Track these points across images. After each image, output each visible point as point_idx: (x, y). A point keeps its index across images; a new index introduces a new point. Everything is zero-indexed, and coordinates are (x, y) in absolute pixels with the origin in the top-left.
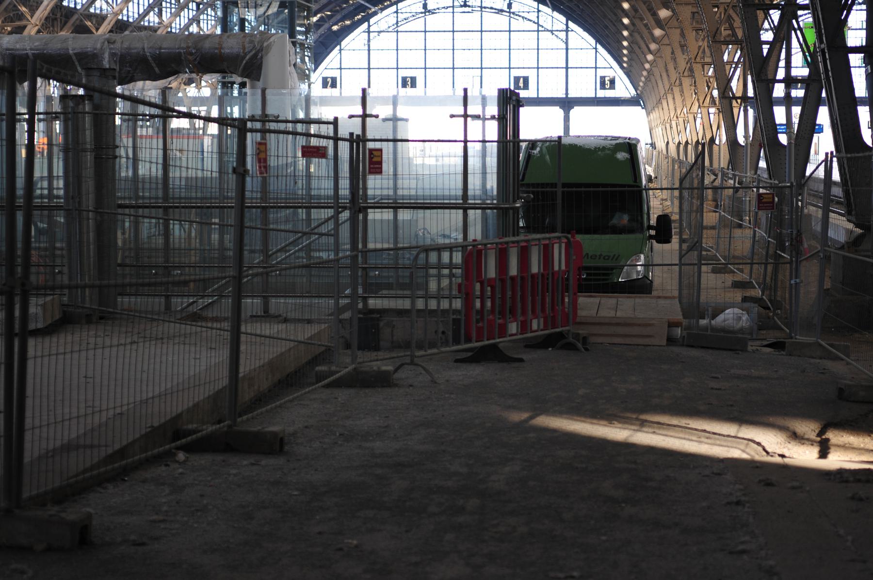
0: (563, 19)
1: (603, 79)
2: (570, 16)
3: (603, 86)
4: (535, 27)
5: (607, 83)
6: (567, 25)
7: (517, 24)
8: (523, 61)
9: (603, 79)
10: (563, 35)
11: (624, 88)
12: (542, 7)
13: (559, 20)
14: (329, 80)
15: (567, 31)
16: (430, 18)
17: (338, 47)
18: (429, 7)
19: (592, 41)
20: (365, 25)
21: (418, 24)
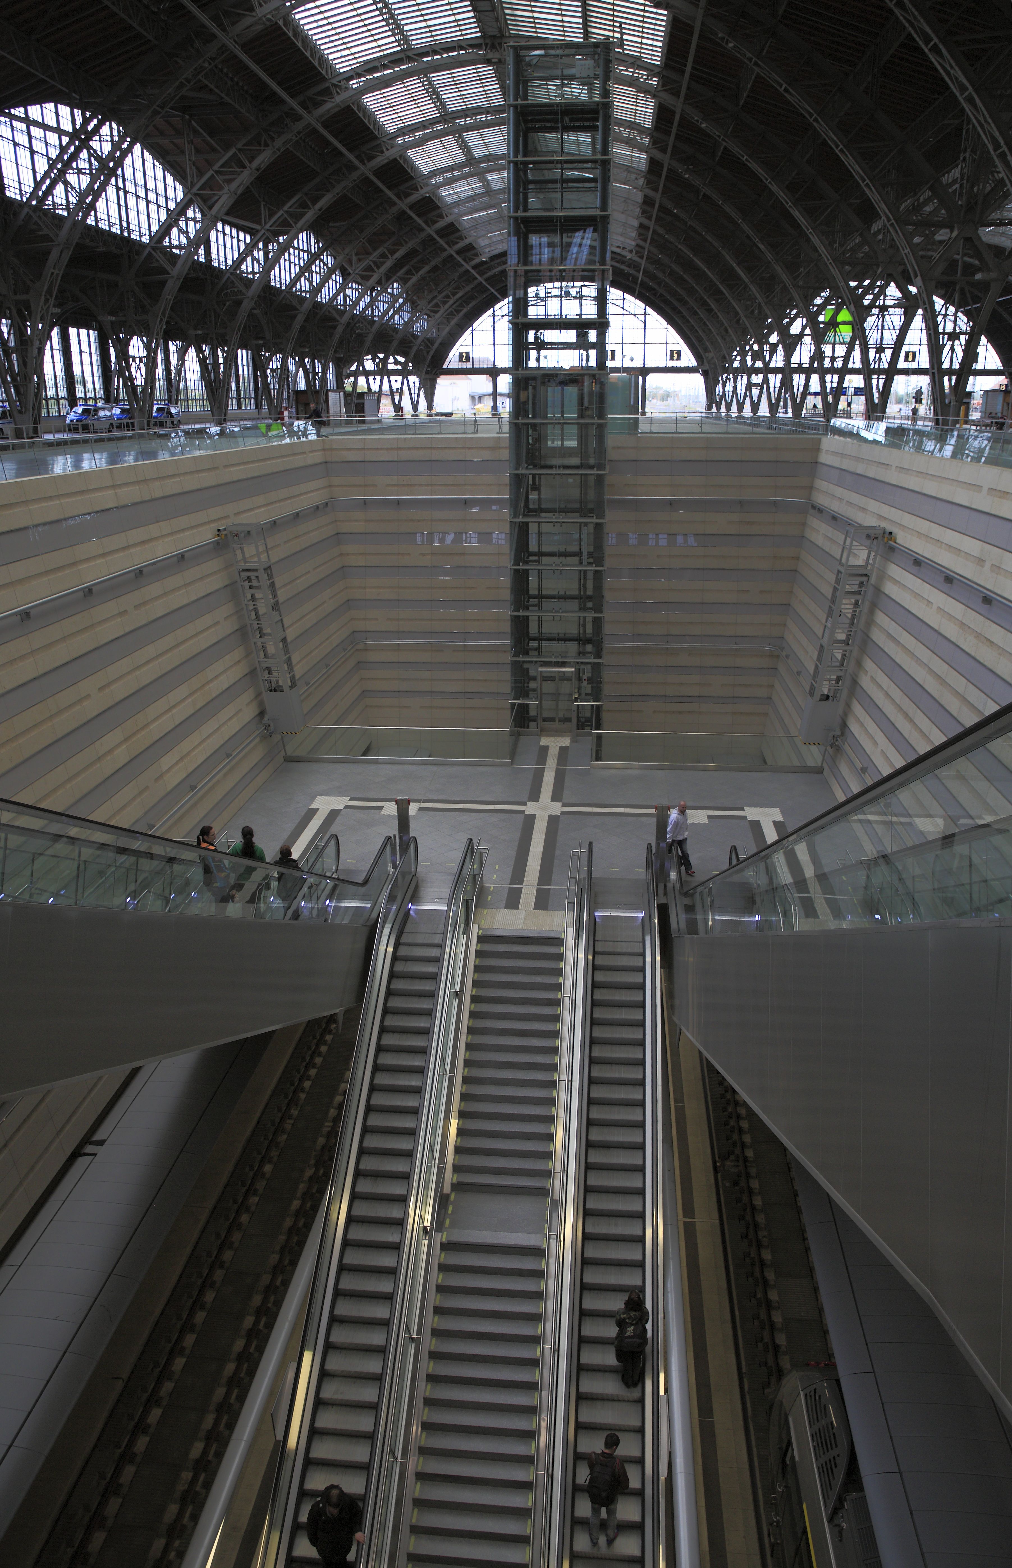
0: (642, 305)
1: (672, 352)
2: (648, 302)
3: (672, 358)
4: (620, 311)
5: (675, 355)
9: (672, 352)
11: (688, 359)
12: (627, 296)
13: (639, 306)
14: (464, 354)
15: (645, 314)
17: (470, 329)
19: (664, 323)
20: (491, 311)
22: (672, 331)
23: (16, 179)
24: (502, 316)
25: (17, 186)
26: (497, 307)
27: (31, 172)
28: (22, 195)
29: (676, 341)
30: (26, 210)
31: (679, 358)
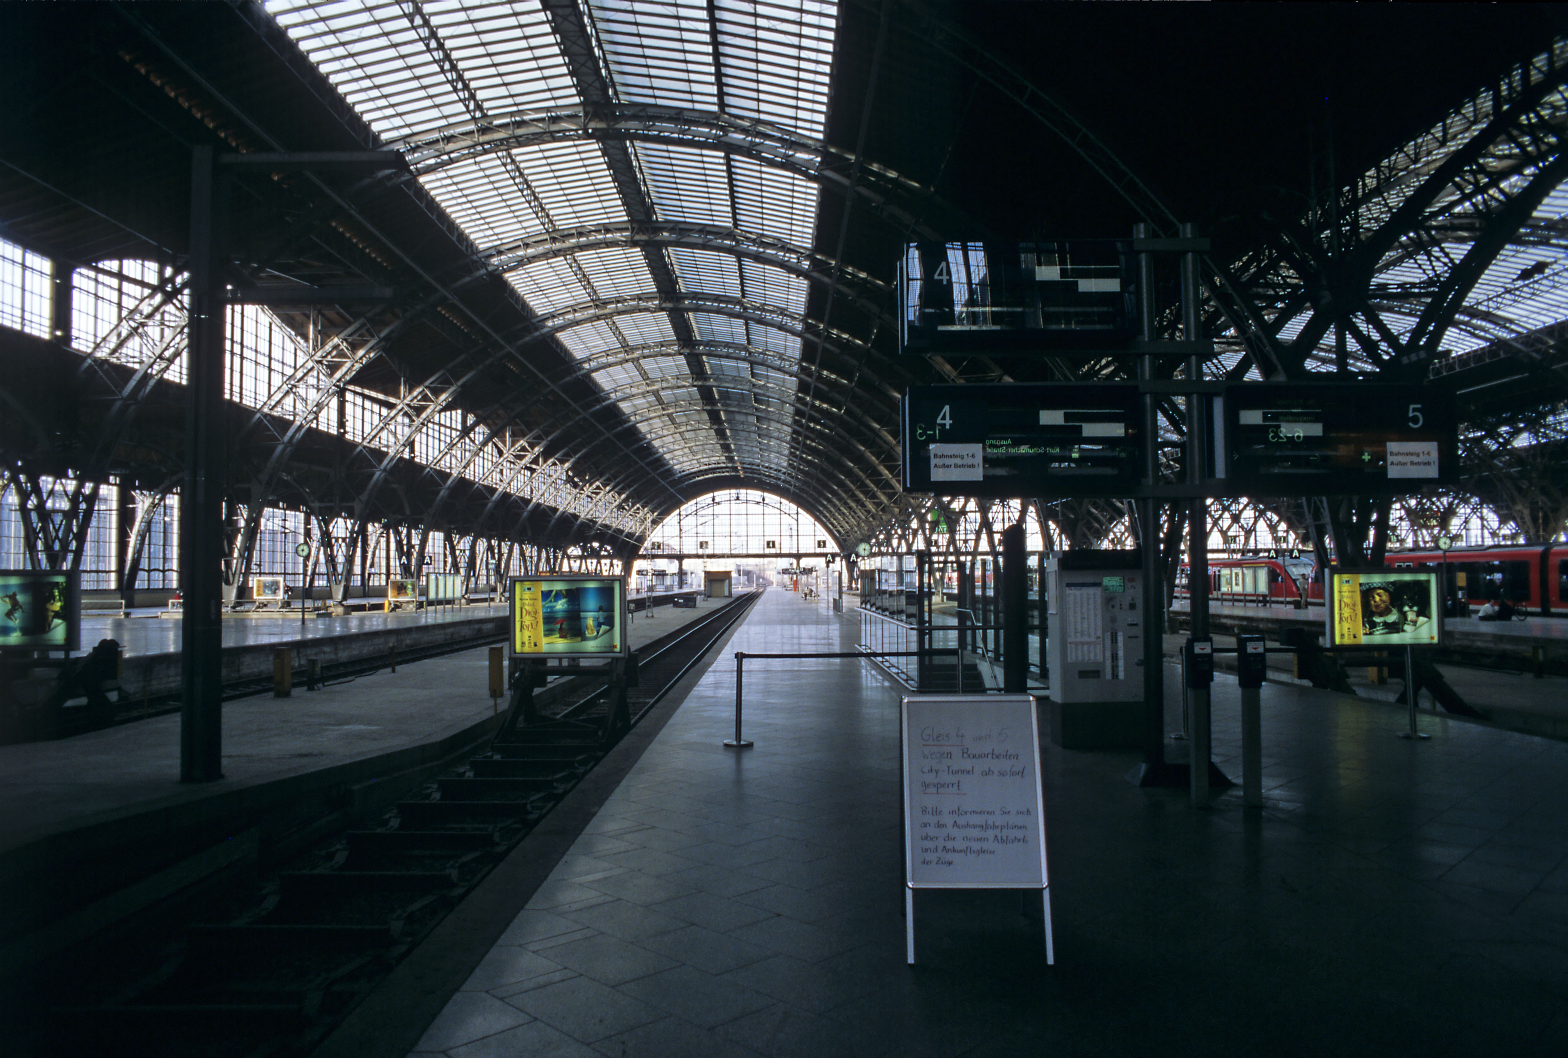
1: (819, 542)
3: (819, 546)
4: (778, 511)
5: (822, 544)
7: (768, 510)
9: (819, 542)
10: (795, 517)
12: (783, 500)
13: (793, 507)
15: (797, 514)
16: (717, 507)
18: (717, 500)
19: (812, 520)
20: (677, 511)
21: (709, 511)
22: (819, 527)
23: (253, 390)
24: (687, 516)
25: (253, 395)
26: (683, 508)
27: (267, 386)
28: (256, 403)
29: (822, 534)
30: (258, 415)
31: (824, 546)
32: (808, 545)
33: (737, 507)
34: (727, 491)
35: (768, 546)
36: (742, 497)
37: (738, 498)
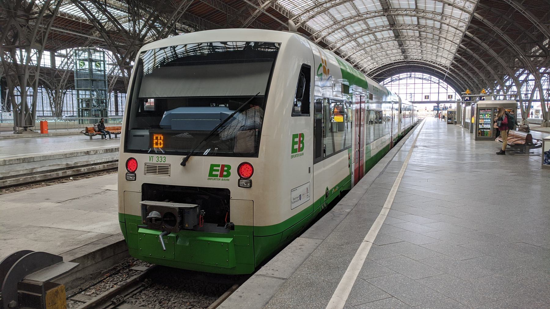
1: (449, 96)
4: (429, 82)
5: (450, 97)
6: (439, 81)
7: (424, 82)
8: (426, 91)
9: (449, 96)
21: (397, 82)
26: (385, 81)
32: (443, 97)
33: (411, 81)
34: (406, 74)
35: (425, 98)
36: (413, 76)
37: (410, 77)
